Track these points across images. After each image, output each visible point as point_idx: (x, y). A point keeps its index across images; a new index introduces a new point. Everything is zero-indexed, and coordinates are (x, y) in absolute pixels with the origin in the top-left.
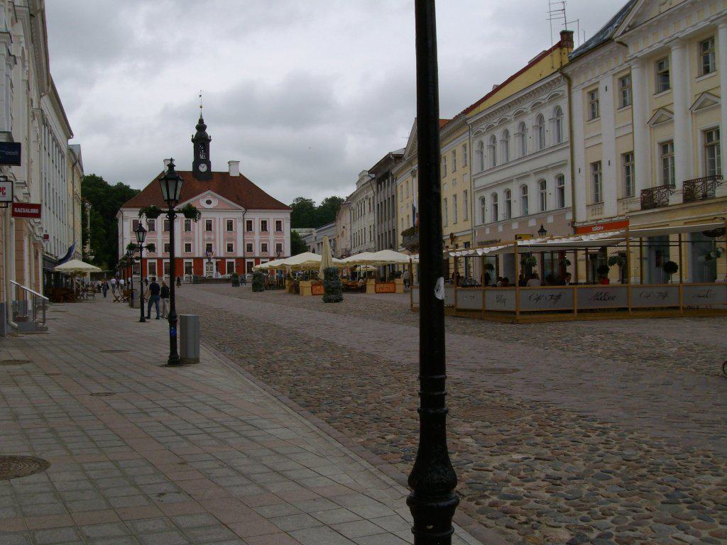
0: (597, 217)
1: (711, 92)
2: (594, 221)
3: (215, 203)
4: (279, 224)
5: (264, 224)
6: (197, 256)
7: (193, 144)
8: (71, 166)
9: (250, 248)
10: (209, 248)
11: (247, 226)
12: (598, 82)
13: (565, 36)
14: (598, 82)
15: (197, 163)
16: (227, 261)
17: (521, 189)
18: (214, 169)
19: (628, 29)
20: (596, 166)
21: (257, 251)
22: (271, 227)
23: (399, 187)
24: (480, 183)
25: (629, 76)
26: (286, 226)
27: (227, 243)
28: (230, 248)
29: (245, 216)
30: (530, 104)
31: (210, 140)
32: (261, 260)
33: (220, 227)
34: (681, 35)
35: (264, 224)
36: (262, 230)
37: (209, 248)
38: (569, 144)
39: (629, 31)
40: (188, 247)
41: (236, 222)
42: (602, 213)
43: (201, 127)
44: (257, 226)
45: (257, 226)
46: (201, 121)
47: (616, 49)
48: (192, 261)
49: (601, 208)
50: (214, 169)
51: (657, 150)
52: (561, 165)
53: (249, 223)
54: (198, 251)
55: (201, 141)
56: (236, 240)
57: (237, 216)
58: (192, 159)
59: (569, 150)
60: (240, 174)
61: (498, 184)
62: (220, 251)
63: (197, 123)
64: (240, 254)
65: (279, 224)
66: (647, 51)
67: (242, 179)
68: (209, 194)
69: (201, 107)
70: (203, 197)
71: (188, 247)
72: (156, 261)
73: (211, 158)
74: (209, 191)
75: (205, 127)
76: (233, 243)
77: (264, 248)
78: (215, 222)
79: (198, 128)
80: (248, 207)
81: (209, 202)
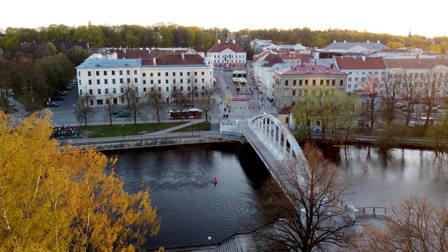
9: (237, 62)
22: (242, 57)
44: (238, 57)
45: (238, 57)
64: (234, 63)
68: (228, 49)
80: (236, 52)
81: (228, 51)
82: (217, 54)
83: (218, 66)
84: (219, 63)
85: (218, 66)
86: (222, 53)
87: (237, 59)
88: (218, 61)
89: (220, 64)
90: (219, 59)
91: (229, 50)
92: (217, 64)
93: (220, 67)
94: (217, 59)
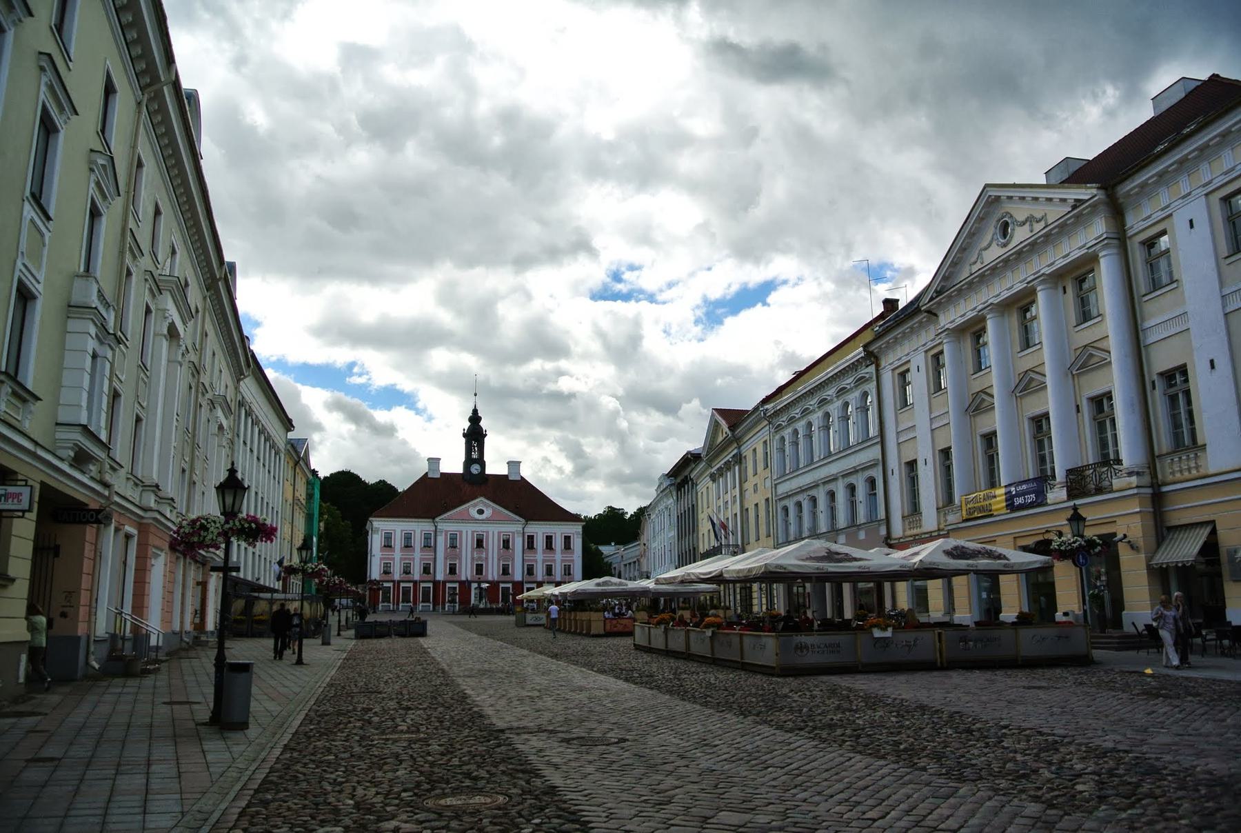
0: (915, 531)
1: (1036, 370)
2: (911, 536)
3: (488, 513)
4: (567, 539)
5: (549, 539)
6: (463, 578)
7: (463, 440)
8: (291, 464)
10: (479, 569)
11: (528, 542)
12: (909, 361)
13: (890, 306)
14: (909, 361)
16: (502, 585)
17: (828, 497)
18: (489, 471)
19: (935, 294)
20: (912, 465)
21: (540, 574)
22: (558, 543)
23: (699, 494)
24: (783, 489)
25: (941, 352)
26: (577, 544)
27: (502, 563)
28: (505, 571)
29: (526, 530)
30: (833, 390)
32: (526, 586)
33: (493, 545)
34: (996, 301)
35: (549, 539)
36: (547, 548)
37: (479, 569)
38: (879, 439)
39: (937, 297)
40: (453, 570)
42: (920, 527)
44: (540, 543)
45: (540, 543)
46: (475, 411)
47: (925, 319)
48: (457, 585)
49: (920, 520)
50: (489, 471)
51: (979, 444)
52: (873, 465)
53: (531, 538)
54: (466, 572)
55: (475, 436)
56: (513, 559)
57: (514, 528)
58: (463, 458)
59: (879, 447)
61: (802, 491)
62: (492, 573)
64: (518, 577)
65: (567, 539)
66: (959, 321)
67: (524, 486)
68: (481, 502)
69: (476, 395)
70: (475, 506)
71: (453, 570)
72: (411, 585)
73: (487, 457)
75: (479, 419)
76: (510, 563)
77: (549, 571)
79: (471, 420)
81: (481, 512)
82: (418, 528)
83: (426, 599)
84: (427, 577)
85: (426, 599)
86: (446, 525)
87: (529, 556)
88: (426, 570)
89: (436, 583)
90: (429, 555)
91: (490, 509)
92: (415, 583)
93: (435, 603)
94: (418, 558)
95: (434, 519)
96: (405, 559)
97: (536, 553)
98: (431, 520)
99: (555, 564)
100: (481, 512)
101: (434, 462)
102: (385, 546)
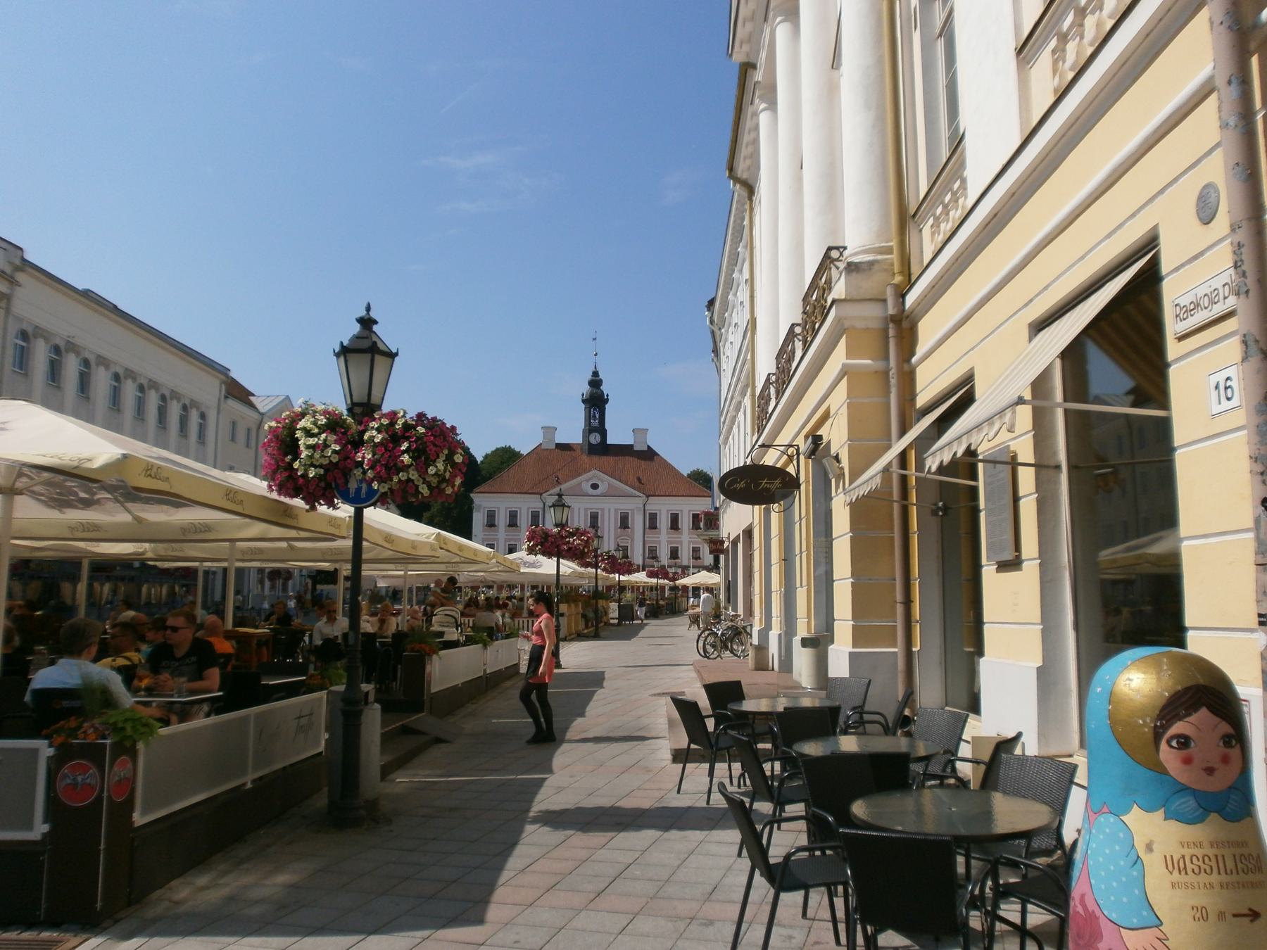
15: (589, 430)
18: (612, 439)
21: (685, 557)
29: (646, 508)
31: (607, 400)
36: (672, 528)
41: (633, 515)
43: (595, 382)
44: (664, 522)
45: (664, 522)
46: (596, 374)
50: (612, 439)
53: (653, 518)
55: (596, 402)
56: (632, 540)
57: (633, 504)
60: (648, 446)
63: (589, 376)
70: (587, 481)
73: (607, 426)
74: (594, 472)
77: (674, 554)
78: (603, 515)
81: (595, 486)
87: (651, 536)
95: (541, 494)
96: (510, 540)
97: (659, 533)
98: (538, 496)
99: (681, 545)
100: (595, 486)
101: (549, 431)
102: (509, 526)
